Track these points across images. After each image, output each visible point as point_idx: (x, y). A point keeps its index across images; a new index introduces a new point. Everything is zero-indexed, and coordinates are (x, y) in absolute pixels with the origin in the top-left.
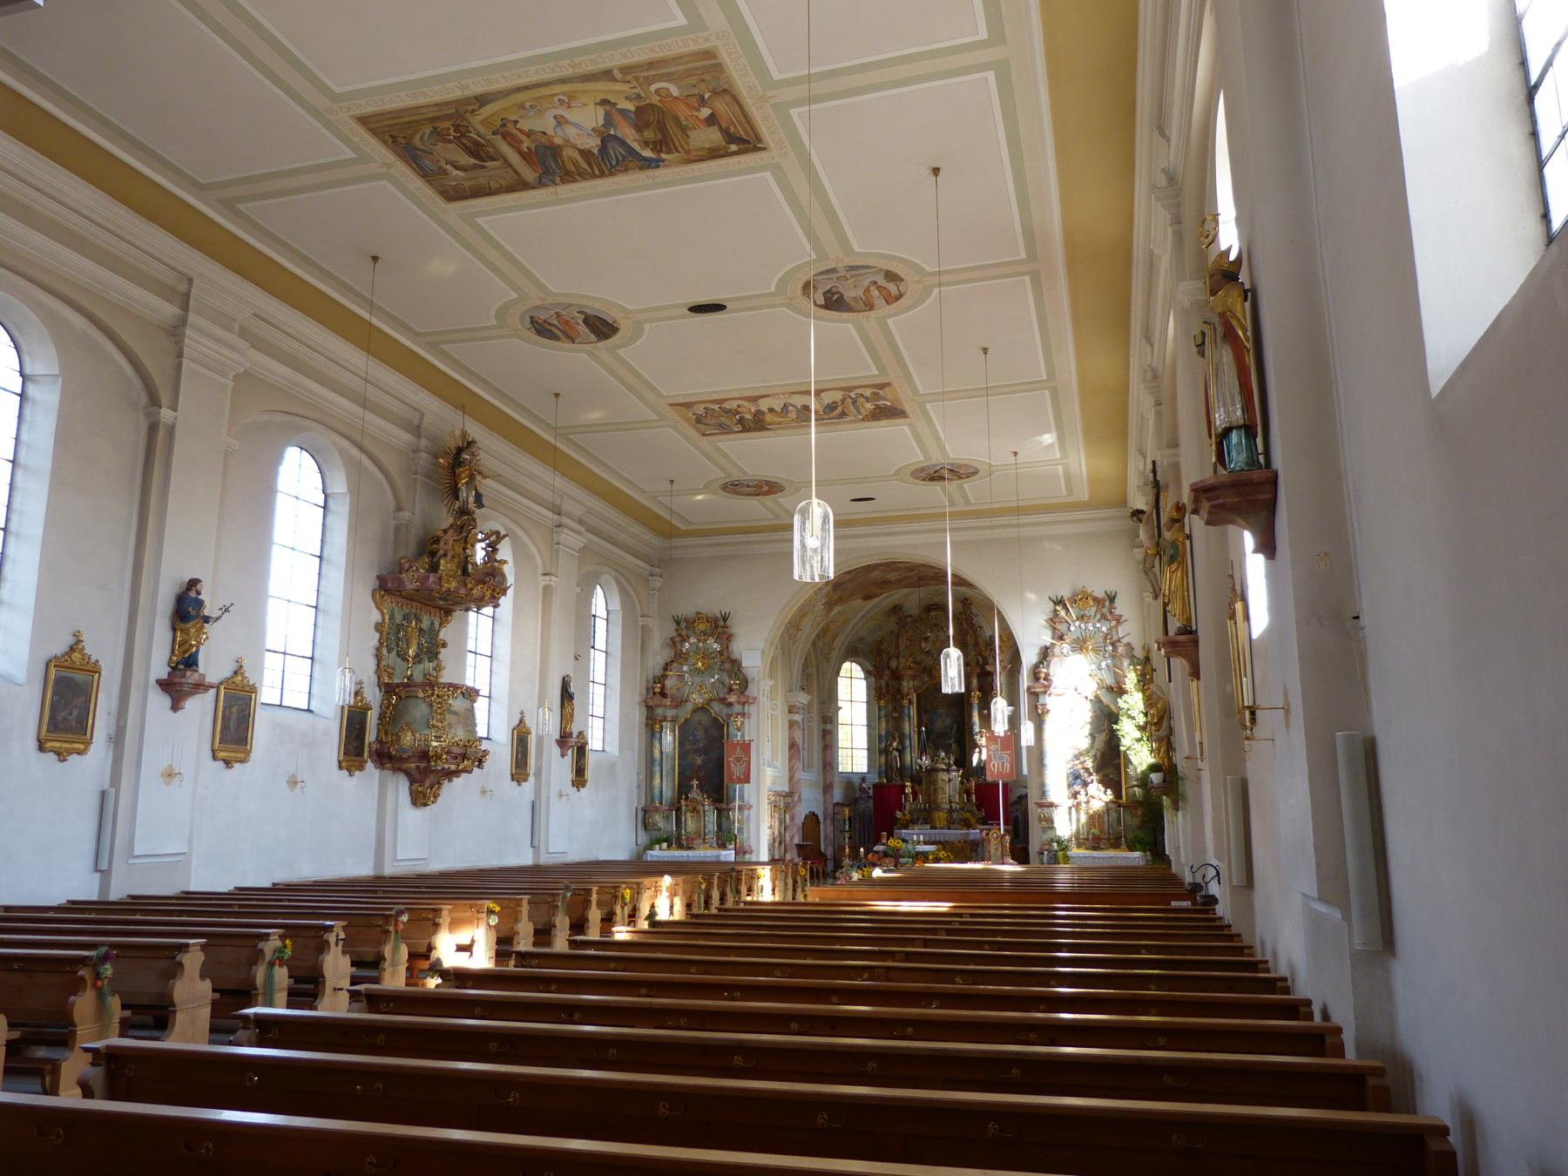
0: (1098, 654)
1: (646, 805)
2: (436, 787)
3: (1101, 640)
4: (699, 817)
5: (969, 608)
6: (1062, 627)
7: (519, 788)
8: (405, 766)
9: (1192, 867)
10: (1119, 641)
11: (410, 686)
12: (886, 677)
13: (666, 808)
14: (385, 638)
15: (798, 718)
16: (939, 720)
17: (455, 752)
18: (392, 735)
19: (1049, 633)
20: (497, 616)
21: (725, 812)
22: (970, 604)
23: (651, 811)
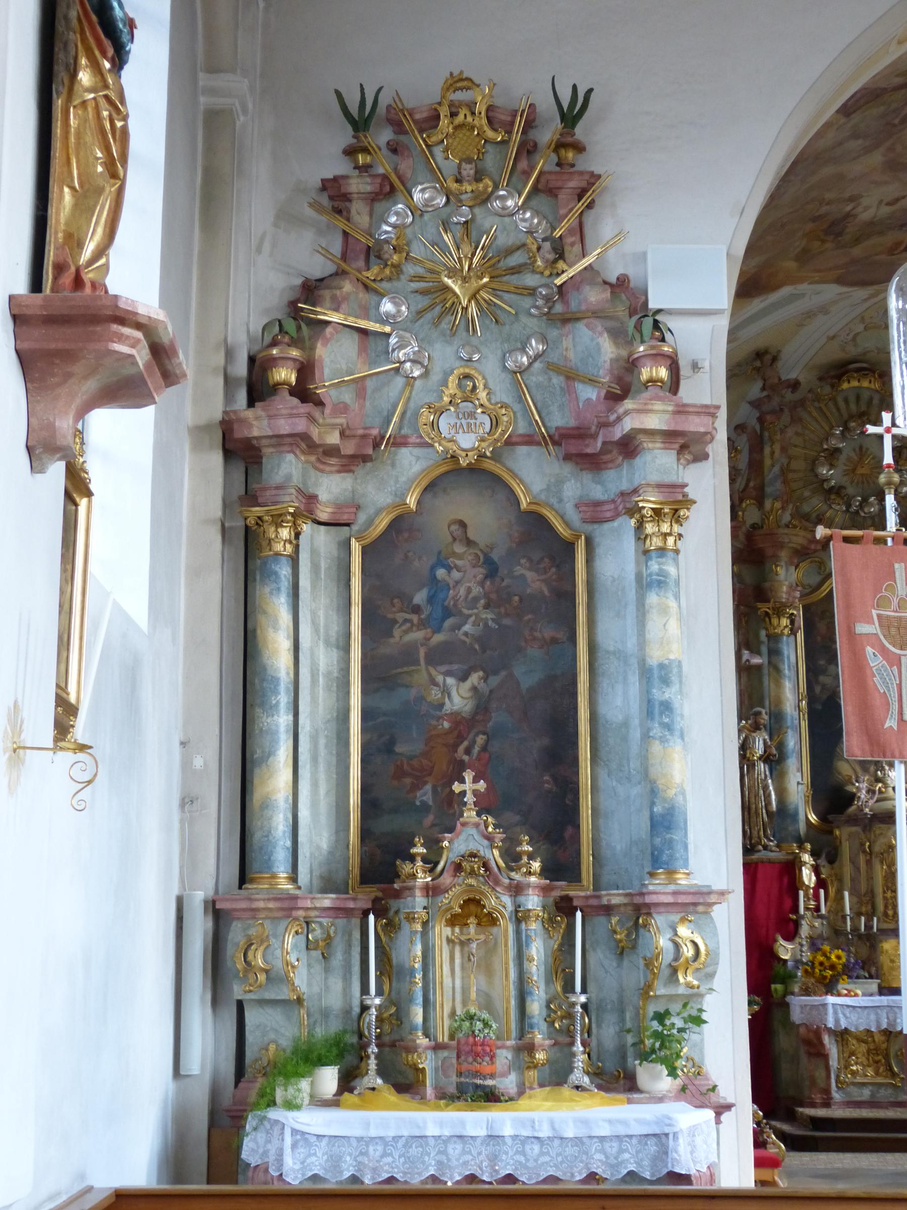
4: (490, 949)
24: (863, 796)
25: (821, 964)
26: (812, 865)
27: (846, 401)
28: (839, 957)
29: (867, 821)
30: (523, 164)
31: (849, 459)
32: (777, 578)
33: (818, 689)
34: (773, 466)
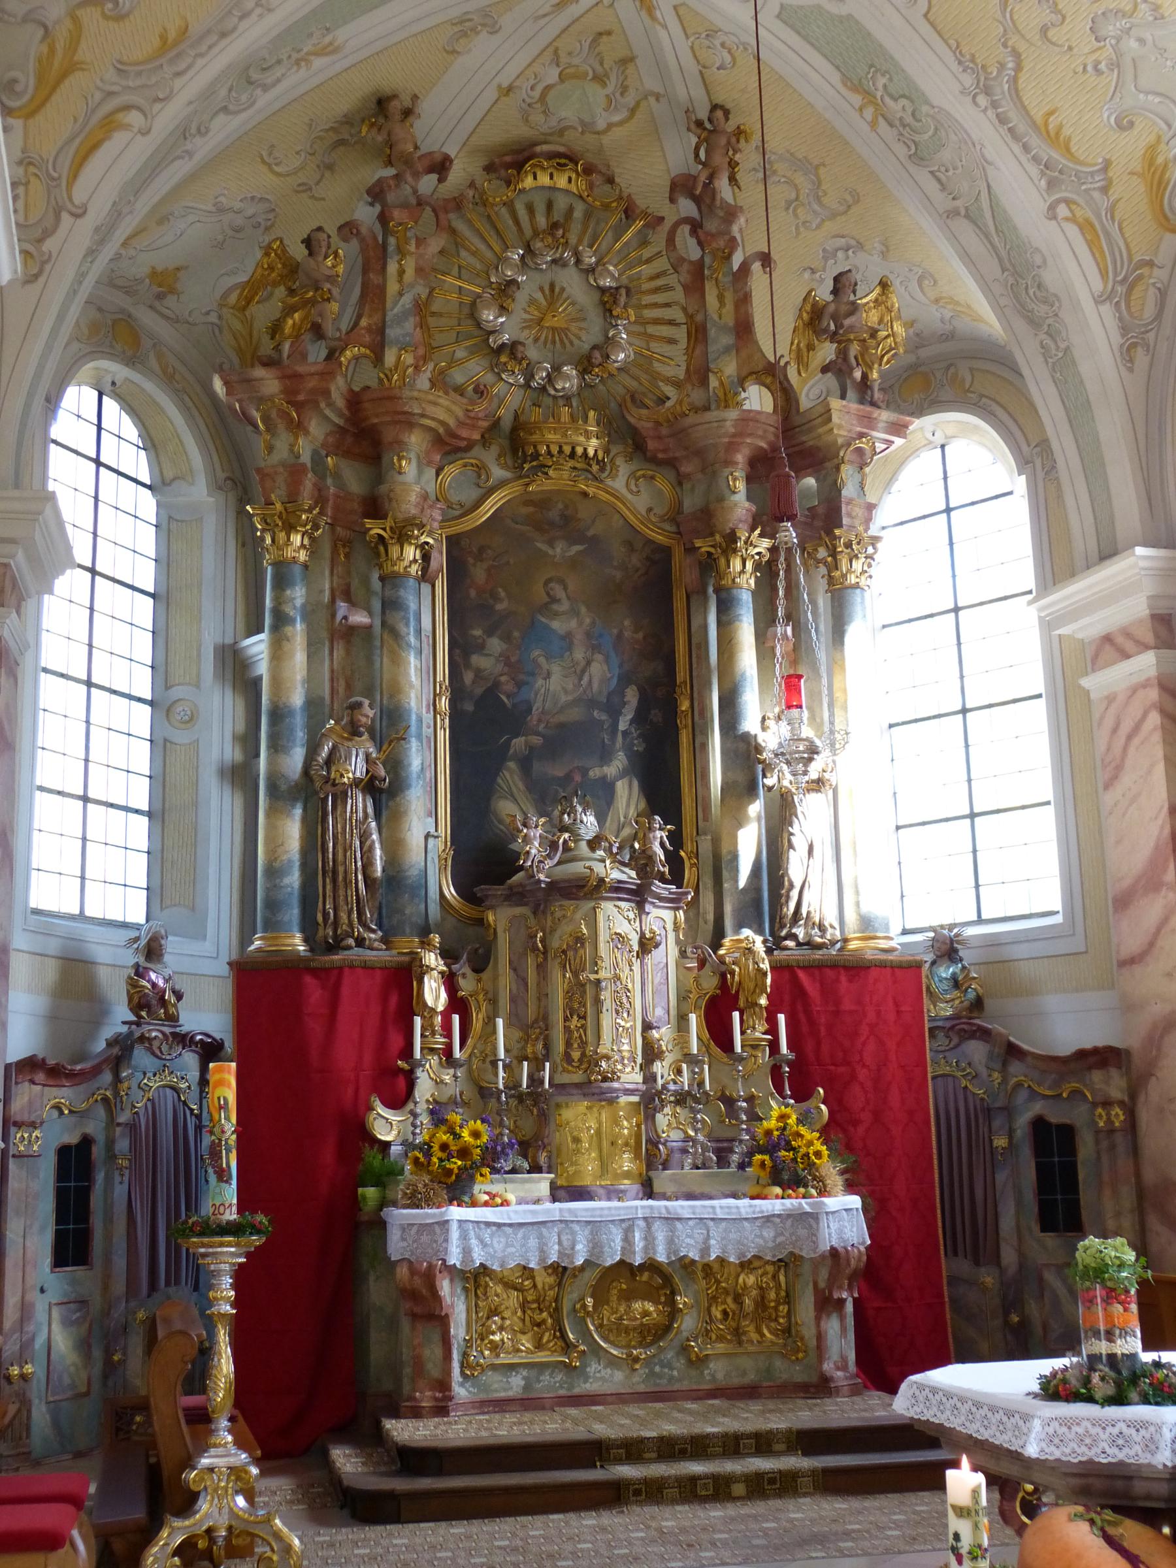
12: (317, 430)
16: (556, 670)
24: (534, 851)
25: (444, 1147)
26: (442, 973)
27: (531, 209)
28: (476, 1134)
29: (540, 895)
31: (532, 302)
32: (401, 478)
33: (468, 677)
34: (401, 294)
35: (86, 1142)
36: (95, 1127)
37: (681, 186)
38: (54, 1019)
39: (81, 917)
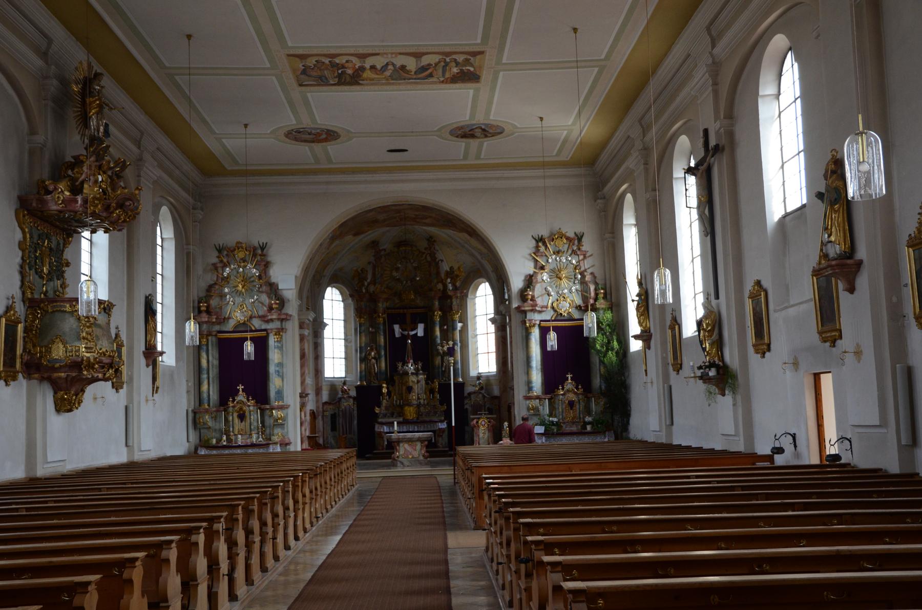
0: (570, 281)
1: (194, 408)
2: (81, 394)
3: (572, 270)
5: (433, 244)
6: (542, 262)
7: (117, 394)
8: (56, 375)
9: (775, 436)
10: (585, 270)
11: (56, 301)
13: (214, 409)
14: (27, 255)
15: (306, 332)
17: (104, 362)
18: (41, 347)
19: (532, 264)
20: (94, 240)
21: (268, 411)
22: (434, 241)
23: (201, 412)
30: (253, 259)
35: (335, 413)
36: (337, 411)
37: (426, 249)
38: (330, 395)
39: (334, 378)
